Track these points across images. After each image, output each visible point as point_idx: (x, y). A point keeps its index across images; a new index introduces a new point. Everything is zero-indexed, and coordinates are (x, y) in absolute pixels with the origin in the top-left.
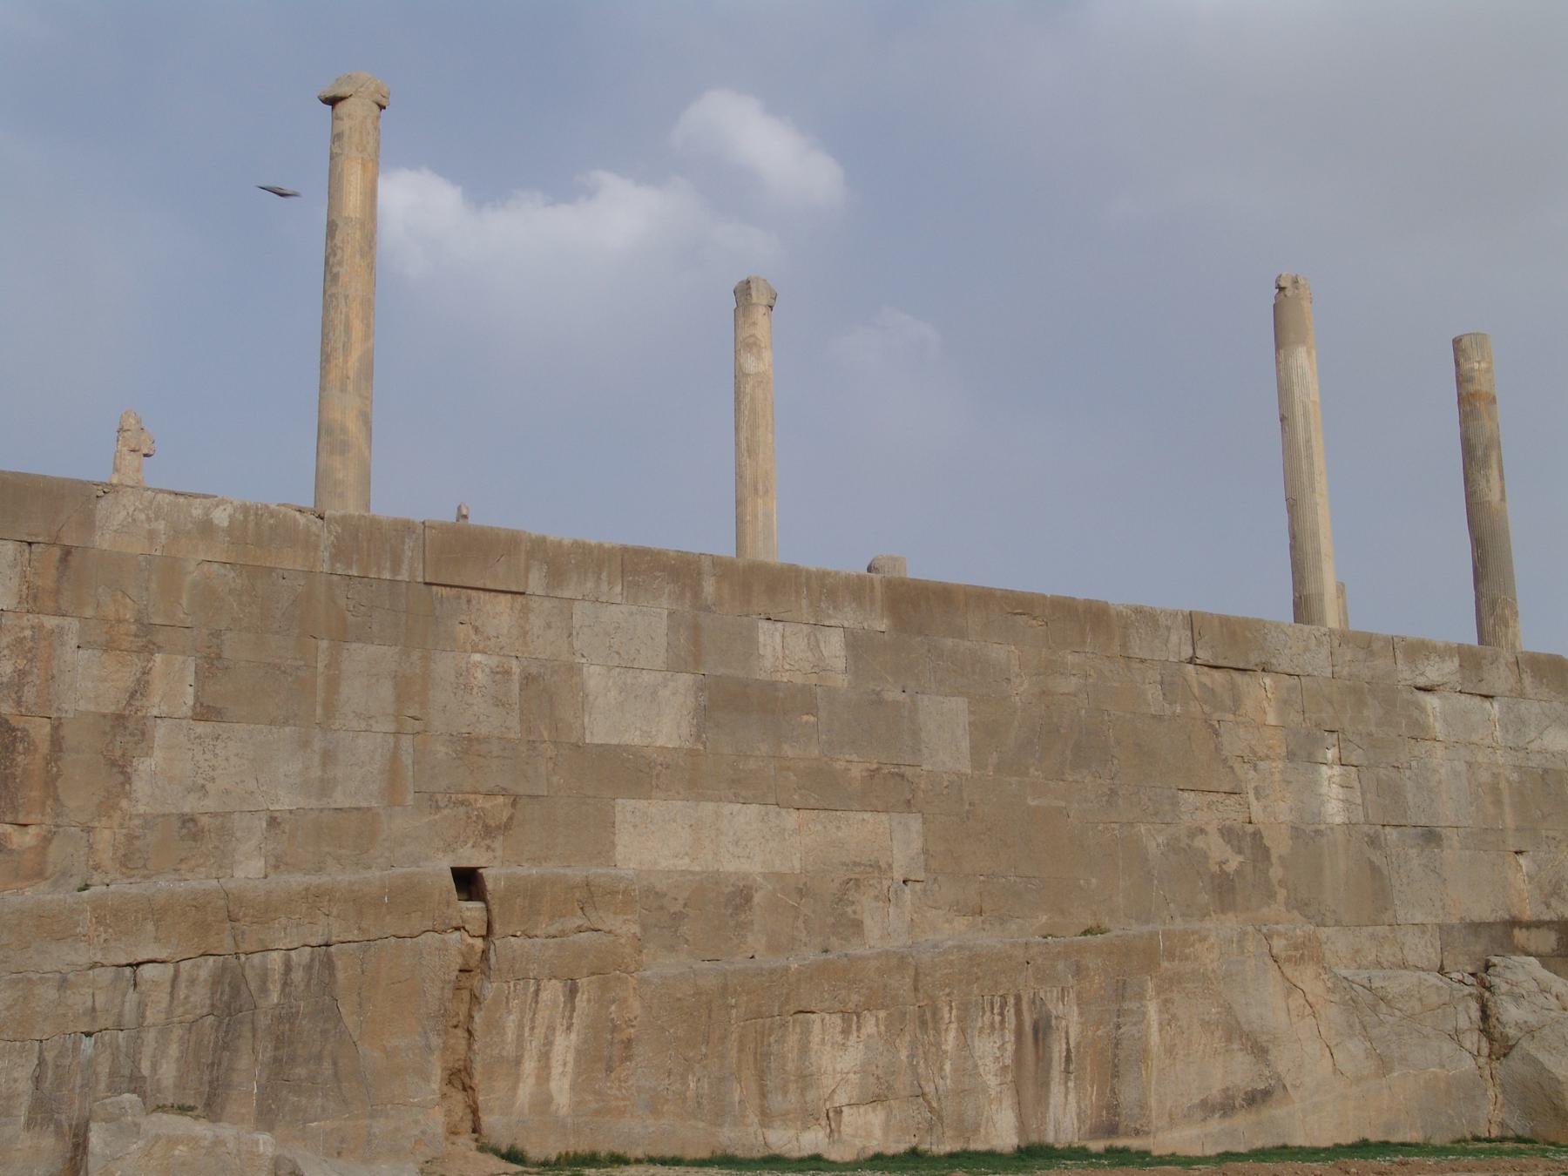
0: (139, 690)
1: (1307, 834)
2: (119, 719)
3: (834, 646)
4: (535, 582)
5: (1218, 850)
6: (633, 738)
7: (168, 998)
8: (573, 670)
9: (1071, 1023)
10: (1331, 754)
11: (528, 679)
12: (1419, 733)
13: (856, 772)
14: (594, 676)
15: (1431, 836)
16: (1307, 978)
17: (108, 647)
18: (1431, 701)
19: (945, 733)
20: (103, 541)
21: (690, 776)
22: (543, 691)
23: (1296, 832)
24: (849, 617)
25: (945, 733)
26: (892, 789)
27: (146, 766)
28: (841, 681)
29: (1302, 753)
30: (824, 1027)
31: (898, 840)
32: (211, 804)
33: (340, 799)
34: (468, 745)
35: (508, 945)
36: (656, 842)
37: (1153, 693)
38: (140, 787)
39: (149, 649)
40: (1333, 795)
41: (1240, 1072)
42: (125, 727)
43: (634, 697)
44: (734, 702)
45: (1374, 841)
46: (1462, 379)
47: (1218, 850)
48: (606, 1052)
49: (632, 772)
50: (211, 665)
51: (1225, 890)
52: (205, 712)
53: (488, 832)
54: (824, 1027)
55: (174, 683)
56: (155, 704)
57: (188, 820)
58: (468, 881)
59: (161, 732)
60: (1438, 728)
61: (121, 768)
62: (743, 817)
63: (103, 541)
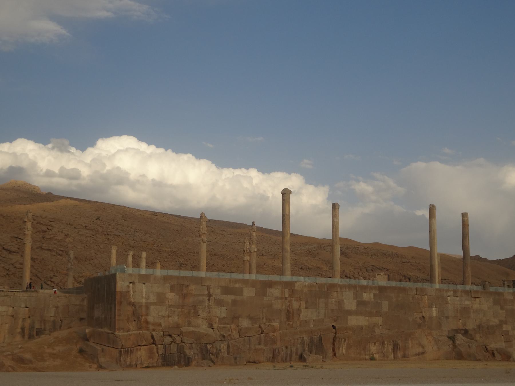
0: (300, 306)
1: (431, 318)
2: (299, 309)
3: (372, 296)
4: (339, 290)
5: (419, 321)
6: (350, 309)
7: (332, 346)
8: (343, 300)
9: (400, 344)
10: (434, 306)
11: (338, 302)
12: (447, 302)
13: (375, 312)
14: (345, 301)
15: (447, 317)
16: (430, 338)
17: (297, 301)
18: (449, 298)
19: (385, 306)
20: (296, 288)
21: (357, 313)
22: (340, 303)
23: (429, 317)
24: (374, 291)
25: (385, 306)
26: (379, 314)
27: (301, 314)
28: (373, 300)
29: (430, 306)
30: (372, 344)
31: (379, 320)
32: (307, 319)
33: (320, 318)
34: (332, 310)
35: (338, 335)
36: (354, 321)
37: (411, 299)
38: (301, 317)
39: (301, 301)
40: (434, 312)
41: (421, 350)
42: (299, 310)
43: (350, 304)
44: (361, 303)
45: (440, 318)
46: (463, 221)
47: (419, 321)
48: (348, 348)
49: (349, 313)
50: (307, 302)
51: (419, 326)
52: (306, 308)
53: (335, 321)
54: (372, 344)
55: (303, 305)
56: (302, 307)
57: (306, 320)
58: (334, 327)
59: (302, 310)
60: (450, 302)
61: (299, 315)
62: (362, 318)
63: (296, 288)
